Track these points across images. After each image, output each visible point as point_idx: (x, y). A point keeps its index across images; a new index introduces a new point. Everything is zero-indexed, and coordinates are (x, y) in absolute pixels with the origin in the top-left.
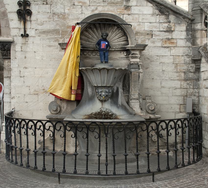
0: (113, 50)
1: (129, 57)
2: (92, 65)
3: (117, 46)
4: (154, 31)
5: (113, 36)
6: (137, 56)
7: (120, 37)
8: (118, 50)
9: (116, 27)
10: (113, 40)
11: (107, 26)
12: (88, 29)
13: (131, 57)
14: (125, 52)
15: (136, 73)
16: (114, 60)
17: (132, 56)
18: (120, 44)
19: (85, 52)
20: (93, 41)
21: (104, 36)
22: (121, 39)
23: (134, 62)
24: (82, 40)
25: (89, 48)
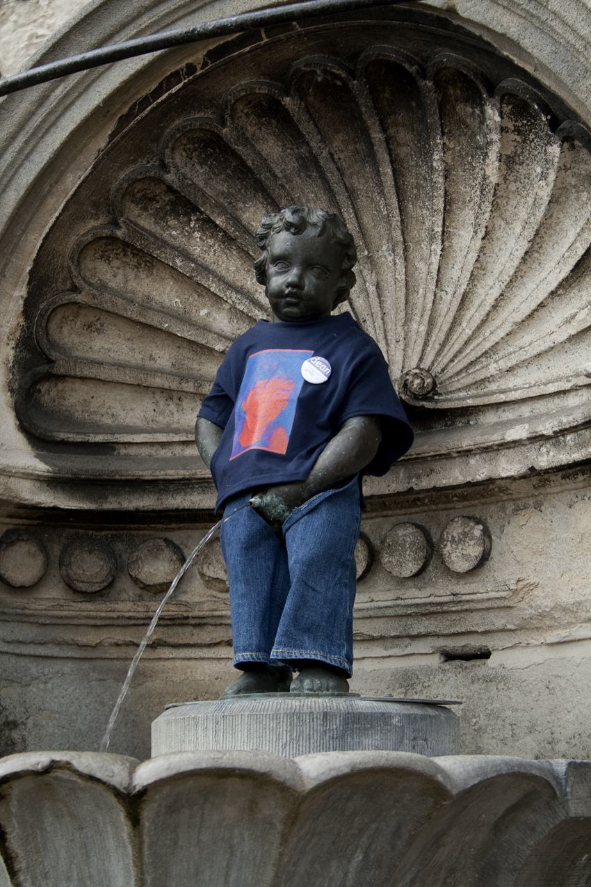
0: (508, 466)
8: (565, 458)
9: (493, 115)
11: (403, 135)
12: (146, 222)
16: (561, 634)
19: (155, 553)
24: (83, 379)
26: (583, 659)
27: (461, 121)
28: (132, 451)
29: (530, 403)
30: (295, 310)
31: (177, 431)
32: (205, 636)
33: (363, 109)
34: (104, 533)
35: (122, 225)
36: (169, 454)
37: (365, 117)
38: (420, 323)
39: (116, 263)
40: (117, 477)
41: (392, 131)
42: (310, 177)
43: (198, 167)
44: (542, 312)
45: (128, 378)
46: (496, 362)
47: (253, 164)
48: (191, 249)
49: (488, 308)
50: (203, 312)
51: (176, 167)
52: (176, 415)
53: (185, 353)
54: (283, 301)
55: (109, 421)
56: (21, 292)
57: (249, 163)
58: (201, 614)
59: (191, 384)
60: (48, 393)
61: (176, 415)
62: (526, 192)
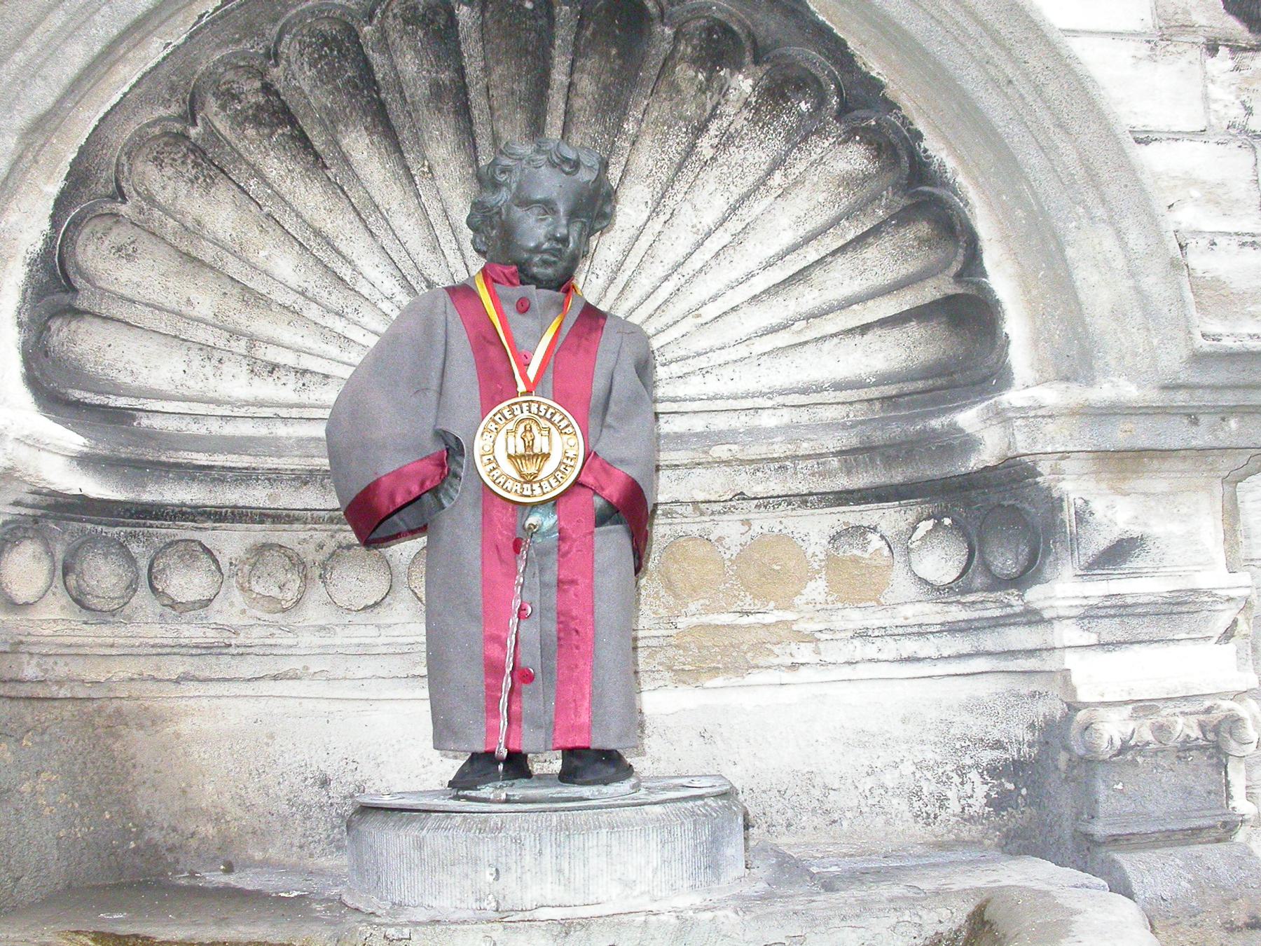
1: (1033, 618)
2: (325, 783)
4: (1204, 243)
6: (1202, 581)
7: (812, 254)
12: (222, 125)
13: (1089, 615)
15: (1231, 928)
17: (1097, 589)
18: (819, 389)
20: (333, 350)
23: (1143, 707)
25: (245, 476)
27: (675, 88)
28: (157, 423)
30: (550, 271)
31: (218, 402)
32: (247, 668)
33: (558, 42)
34: (117, 529)
35: (199, 122)
36: (203, 431)
37: (555, 53)
39: (169, 171)
41: (576, 76)
42: (440, 110)
43: (306, 67)
45: (163, 325)
47: (383, 79)
48: (266, 171)
51: (288, 61)
53: (233, 303)
54: (536, 259)
55: (128, 380)
56: (54, 188)
57: (379, 76)
58: (248, 642)
60: (61, 333)
62: (730, 179)
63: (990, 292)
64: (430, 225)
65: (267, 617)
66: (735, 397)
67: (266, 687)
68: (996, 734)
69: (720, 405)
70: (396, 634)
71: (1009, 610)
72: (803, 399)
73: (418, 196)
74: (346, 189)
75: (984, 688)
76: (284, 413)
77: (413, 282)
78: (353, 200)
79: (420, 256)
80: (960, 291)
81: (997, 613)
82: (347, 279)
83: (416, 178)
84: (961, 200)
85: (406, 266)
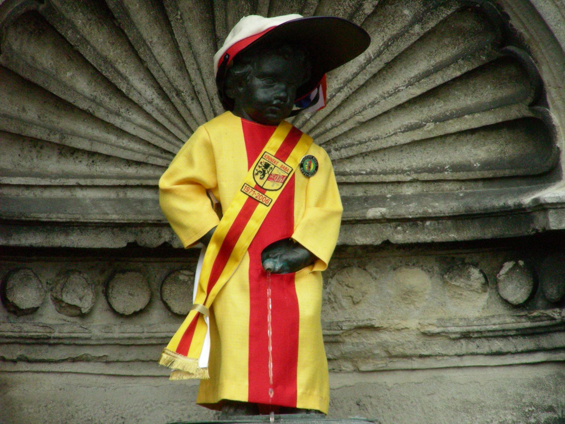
3: (408, 191)
5: (361, 79)
7: (438, 80)
10: (363, 124)
14: (508, 266)
18: (442, 170)
20: (112, 138)
21: (258, 82)
22: (459, 114)
26: (394, 384)
29: (364, 186)
31: (42, 176)
38: (307, 121)
40: (23, 218)
44: (382, 118)
45: (13, 128)
46: (336, 150)
49: (335, 106)
50: (69, 74)
52: (35, 160)
58: (61, 335)
59: (57, 136)
61: (35, 160)
62: (385, 24)
63: (550, 118)
64: (179, 53)
65: (69, 319)
66: (385, 173)
67: (66, 367)
68: (549, 402)
69: (374, 178)
70: (155, 330)
71: (554, 322)
72: (431, 177)
73: (172, 33)
74: (126, 31)
75: (543, 372)
76: (82, 182)
77: (167, 92)
78: (130, 38)
79: (172, 73)
80: (531, 115)
81: (548, 323)
82: (124, 91)
83: (172, 23)
84: (534, 59)
85: (162, 82)
